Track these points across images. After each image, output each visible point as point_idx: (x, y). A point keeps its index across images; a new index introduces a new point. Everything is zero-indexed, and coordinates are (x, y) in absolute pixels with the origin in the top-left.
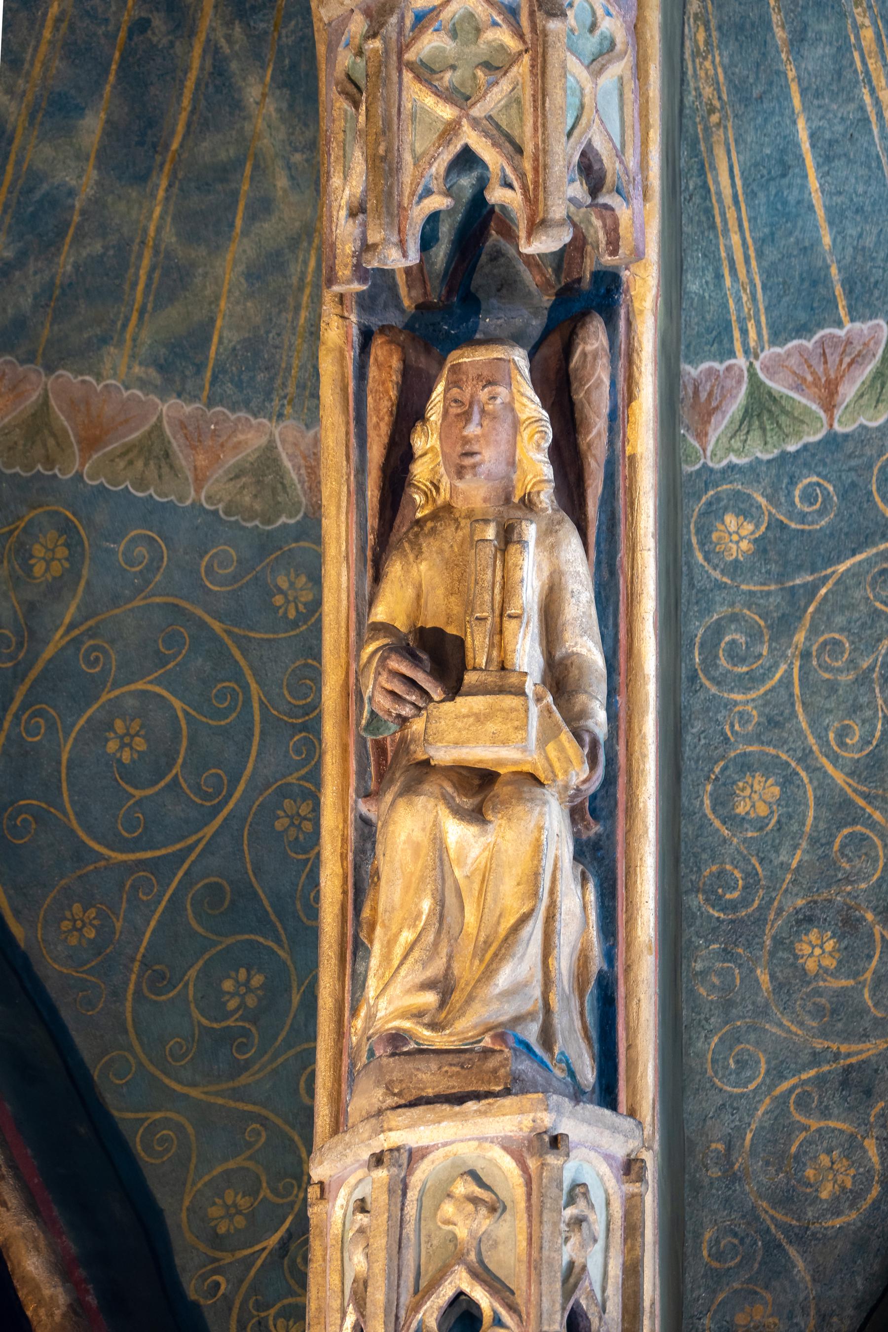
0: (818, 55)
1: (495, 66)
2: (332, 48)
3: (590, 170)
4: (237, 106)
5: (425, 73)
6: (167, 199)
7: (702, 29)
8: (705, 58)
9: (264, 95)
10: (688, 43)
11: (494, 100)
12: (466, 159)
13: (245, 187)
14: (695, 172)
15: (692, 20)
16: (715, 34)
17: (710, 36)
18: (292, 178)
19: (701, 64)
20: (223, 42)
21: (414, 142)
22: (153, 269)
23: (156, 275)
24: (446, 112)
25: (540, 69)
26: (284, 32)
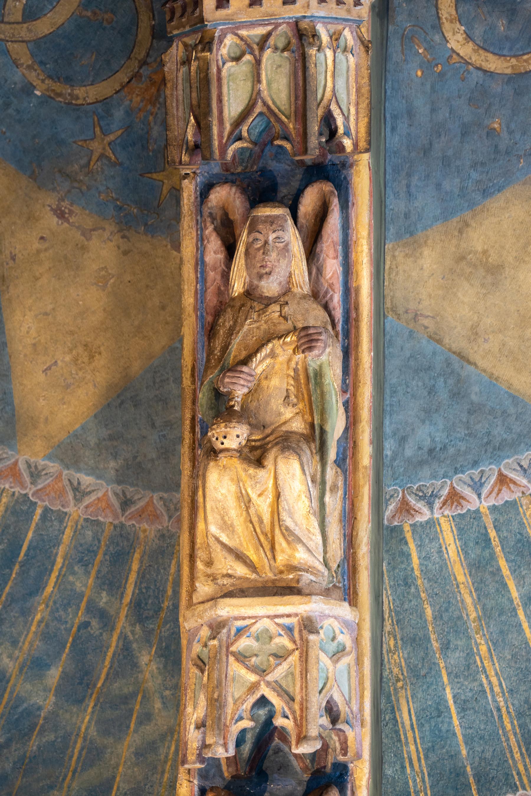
0: (456, 657)
1: (280, 656)
2: (190, 642)
3: (332, 713)
4: (135, 665)
5: (242, 658)
6: (93, 712)
7: (392, 639)
8: (394, 654)
9: (150, 661)
10: (384, 646)
11: (279, 673)
12: (263, 701)
13: (137, 707)
14: (389, 711)
15: (387, 634)
16: (400, 642)
17: (397, 643)
18: (164, 703)
19: (392, 656)
20: (129, 634)
21: (233, 692)
22: (82, 749)
23: (84, 752)
24: (253, 678)
25: (305, 658)
26: (163, 630)
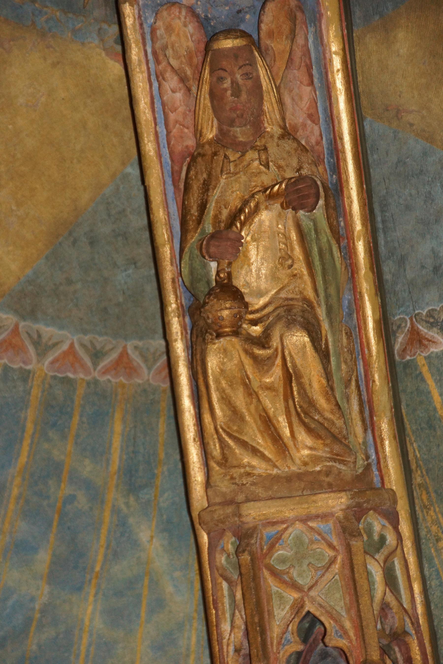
4: (135, 544)
6: (95, 601)
7: (424, 493)
8: (429, 509)
9: (152, 537)
10: (416, 501)
13: (145, 592)
14: (434, 577)
15: (417, 488)
16: (433, 495)
17: (430, 496)
18: (175, 586)
19: (427, 513)
20: (123, 507)
22: (90, 645)
23: (92, 649)
26: (161, 500)
